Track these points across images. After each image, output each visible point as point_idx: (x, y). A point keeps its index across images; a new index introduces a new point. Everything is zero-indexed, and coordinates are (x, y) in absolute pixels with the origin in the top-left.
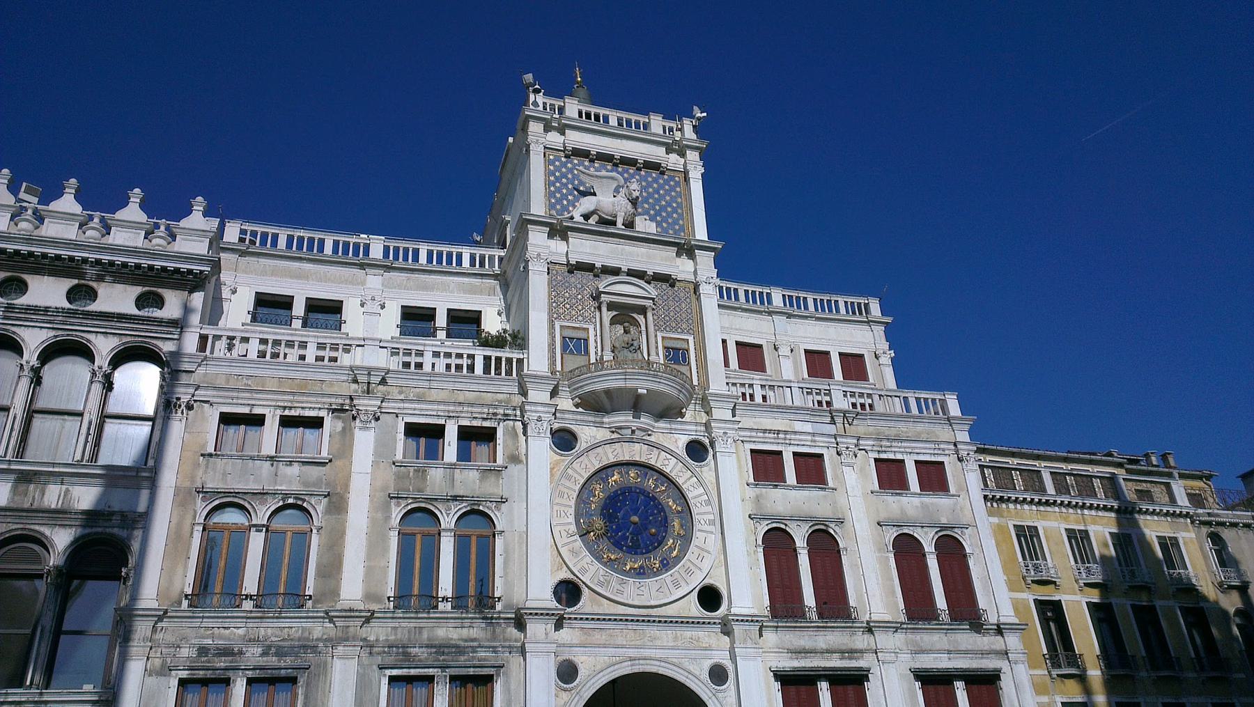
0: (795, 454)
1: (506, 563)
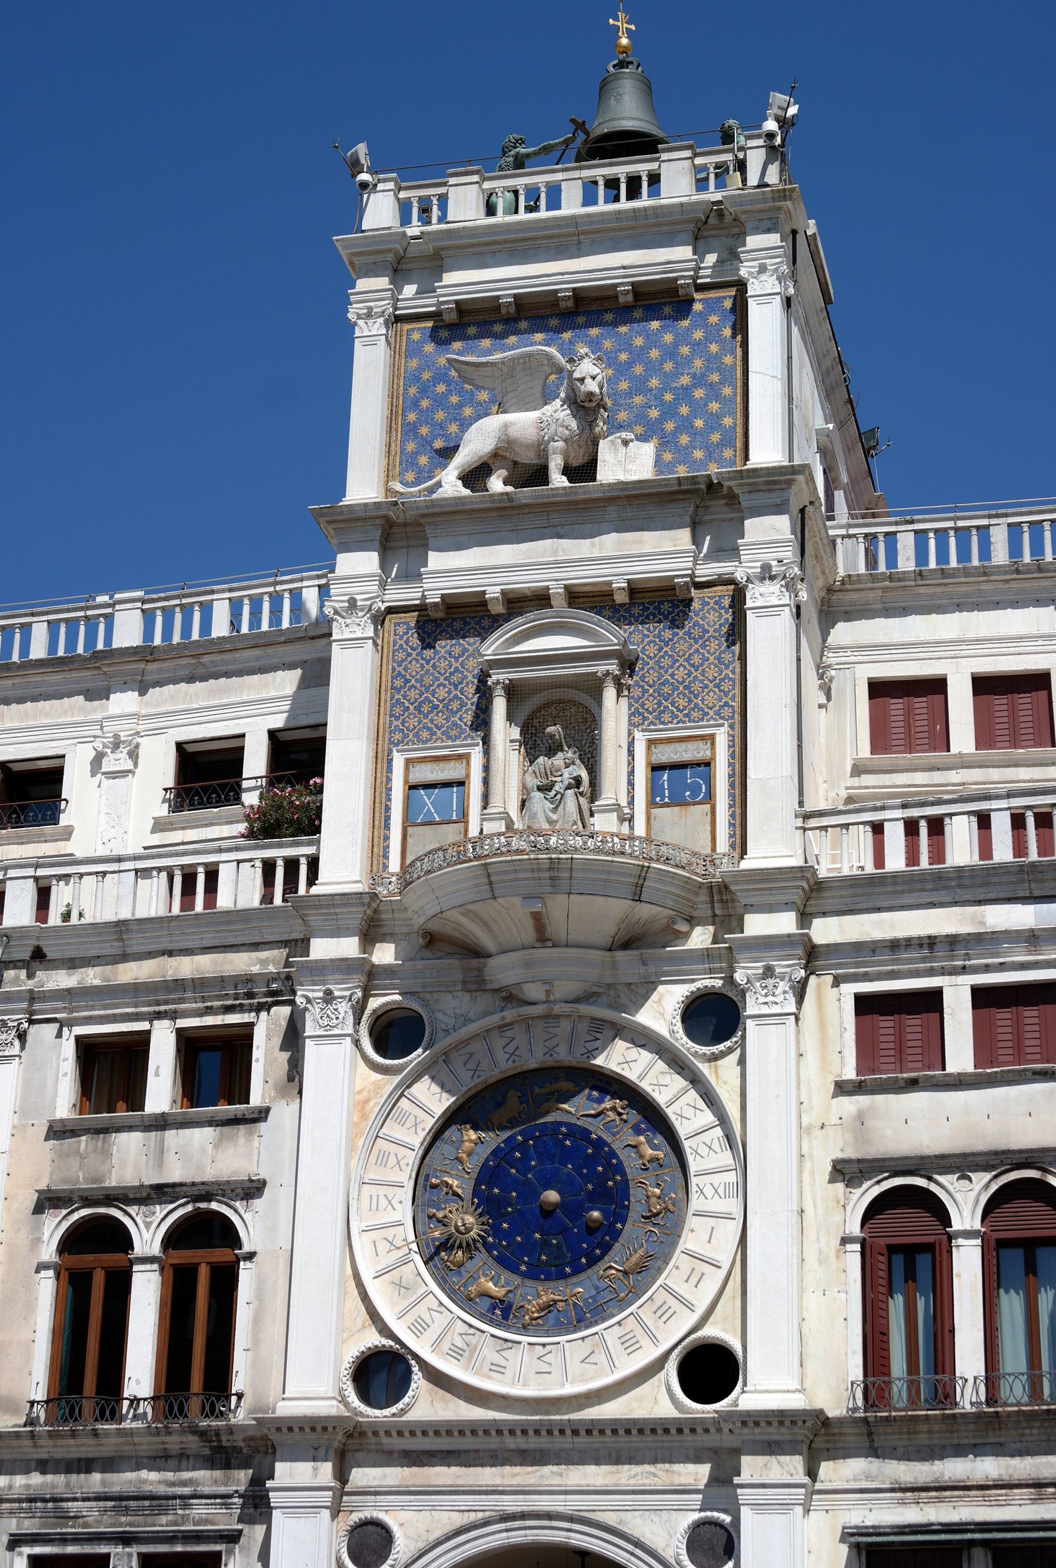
1: (257, 1320)
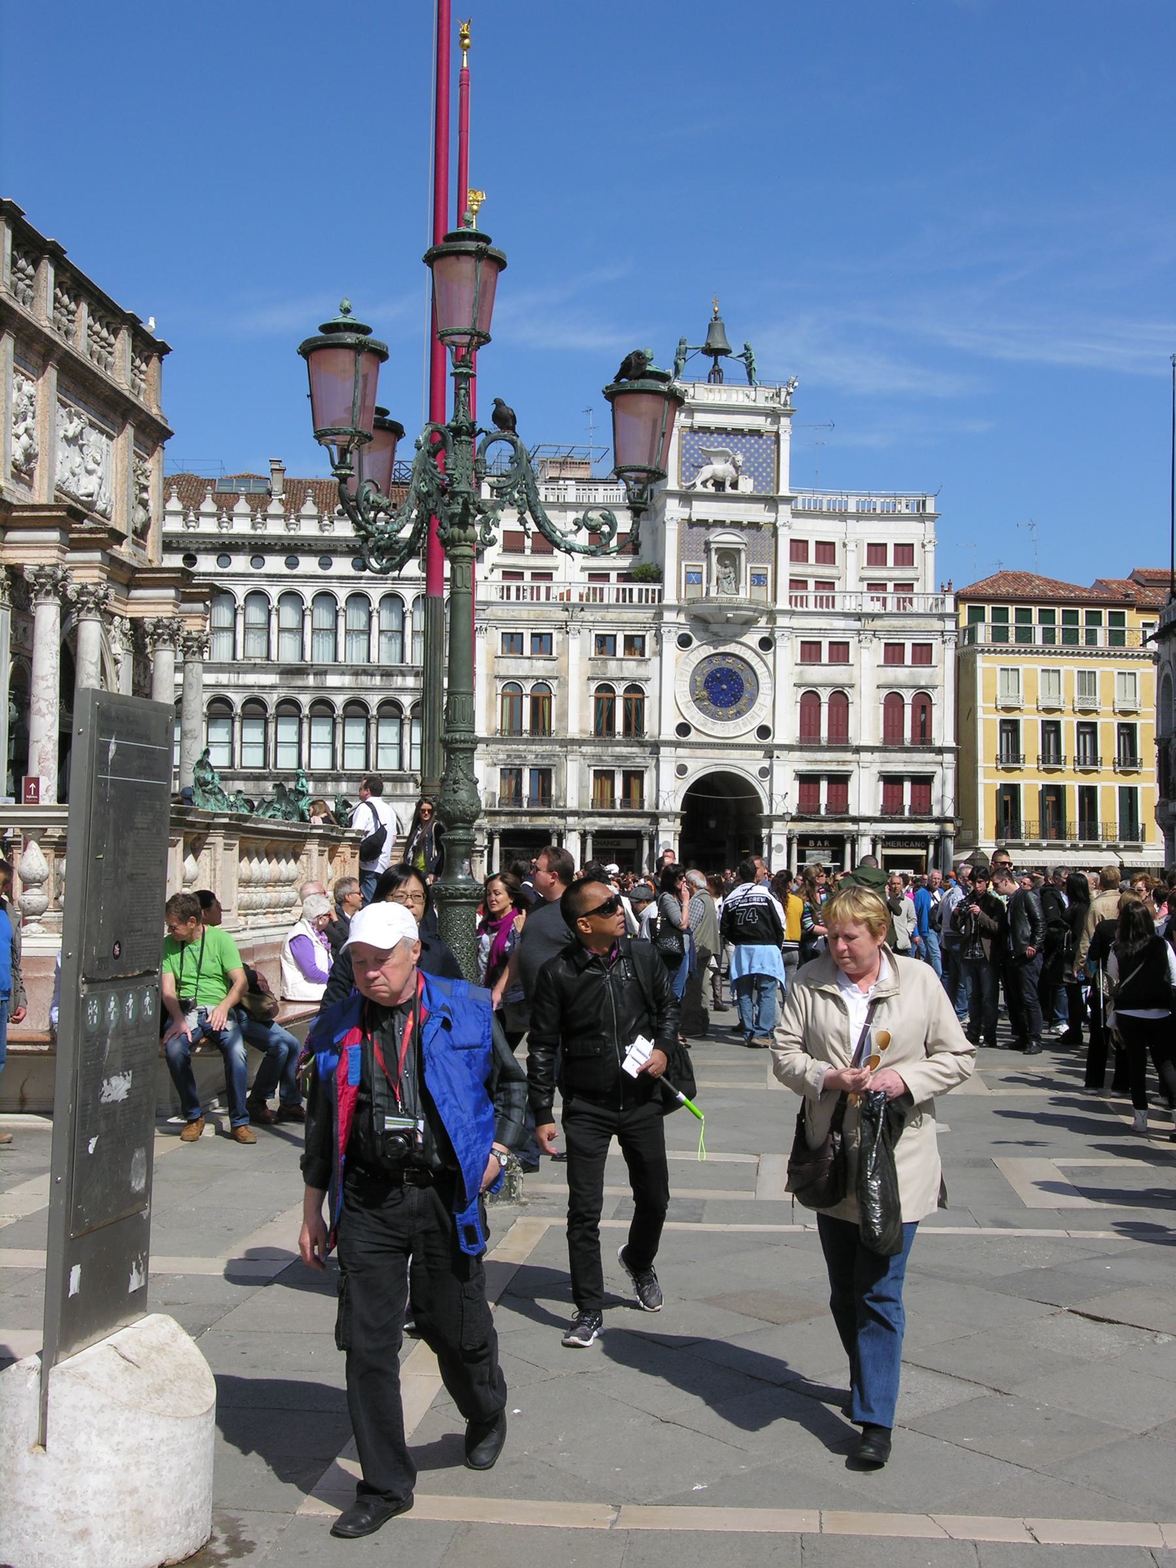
0: (831, 643)
1: (650, 713)
